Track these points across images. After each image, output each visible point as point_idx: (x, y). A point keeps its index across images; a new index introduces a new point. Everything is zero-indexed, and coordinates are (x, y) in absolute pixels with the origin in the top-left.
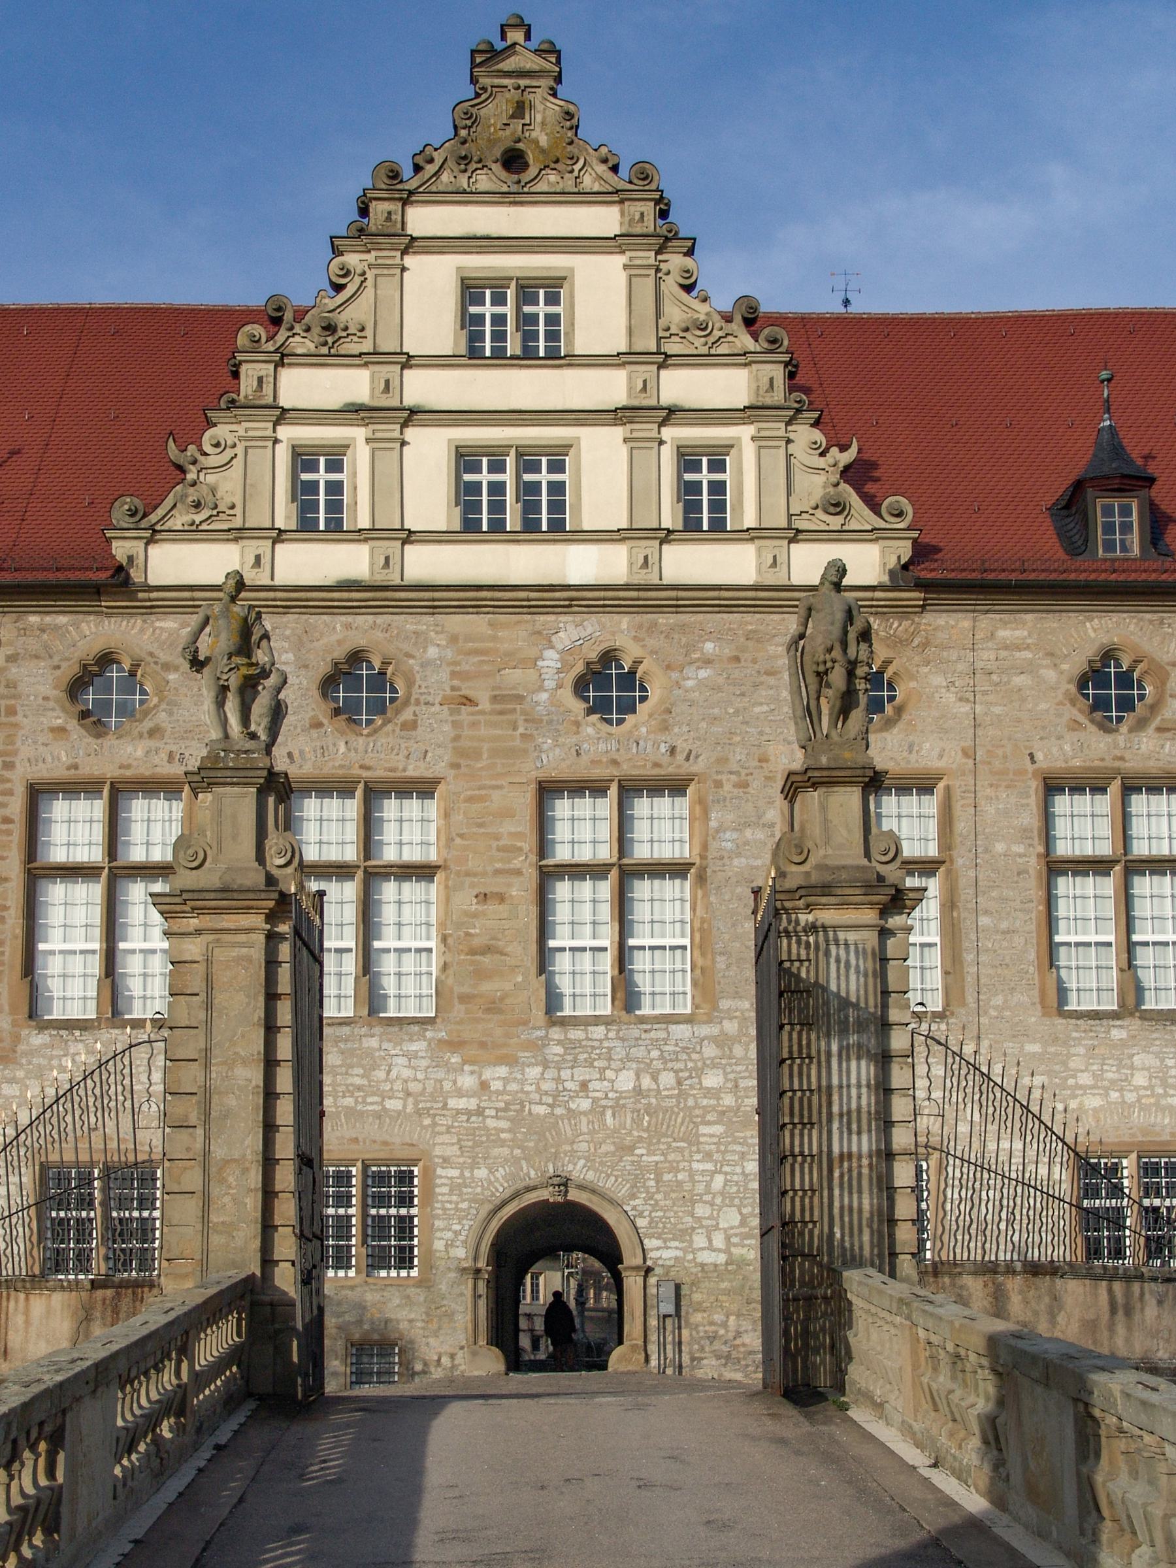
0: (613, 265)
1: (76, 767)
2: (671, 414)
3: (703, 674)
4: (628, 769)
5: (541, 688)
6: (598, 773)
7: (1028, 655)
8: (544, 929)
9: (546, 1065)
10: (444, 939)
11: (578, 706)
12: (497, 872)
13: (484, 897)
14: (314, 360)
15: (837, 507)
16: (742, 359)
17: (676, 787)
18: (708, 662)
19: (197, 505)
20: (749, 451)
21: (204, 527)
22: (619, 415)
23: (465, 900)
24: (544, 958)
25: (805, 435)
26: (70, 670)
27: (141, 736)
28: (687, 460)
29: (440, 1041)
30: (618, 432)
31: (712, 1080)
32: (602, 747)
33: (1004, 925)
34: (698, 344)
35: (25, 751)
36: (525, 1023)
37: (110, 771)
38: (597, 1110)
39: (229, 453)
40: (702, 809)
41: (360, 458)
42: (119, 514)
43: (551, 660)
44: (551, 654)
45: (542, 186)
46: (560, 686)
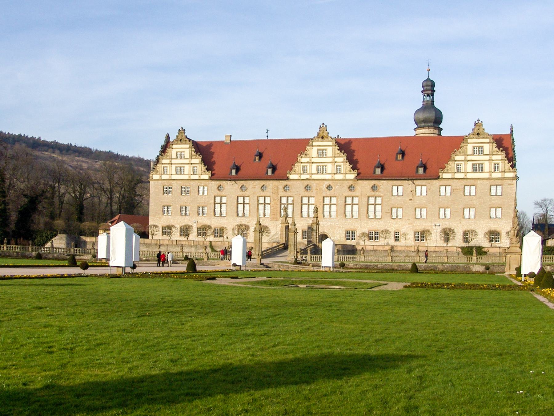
0: (331, 147)
2: (335, 162)
4: (331, 196)
8: (323, 210)
11: (326, 190)
14: (305, 157)
15: (350, 171)
16: (342, 157)
17: (335, 197)
22: (331, 162)
24: (323, 212)
25: (348, 164)
26: (284, 186)
28: (337, 166)
30: (331, 164)
31: (337, 223)
34: (338, 155)
35: (280, 193)
37: (287, 195)
38: (327, 226)
40: (337, 199)
41: (308, 167)
42: (288, 172)
43: (324, 185)
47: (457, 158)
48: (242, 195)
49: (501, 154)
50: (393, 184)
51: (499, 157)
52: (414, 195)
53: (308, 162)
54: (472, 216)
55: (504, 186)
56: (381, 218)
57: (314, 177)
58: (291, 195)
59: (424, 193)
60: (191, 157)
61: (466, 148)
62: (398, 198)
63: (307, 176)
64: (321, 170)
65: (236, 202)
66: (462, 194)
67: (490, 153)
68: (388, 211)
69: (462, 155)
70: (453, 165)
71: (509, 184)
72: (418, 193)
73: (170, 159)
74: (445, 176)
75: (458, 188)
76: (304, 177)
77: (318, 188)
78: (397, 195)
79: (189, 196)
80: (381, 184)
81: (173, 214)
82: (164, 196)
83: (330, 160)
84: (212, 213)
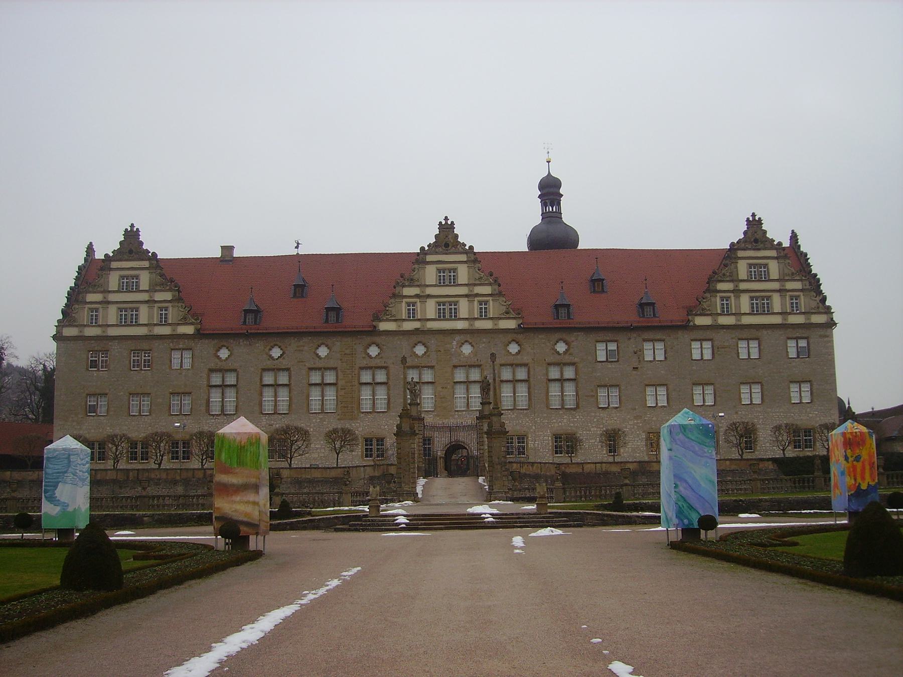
1: (367, 364)
2: (477, 295)
3: (483, 345)
4: (469, 363)
5: (453, 348)
6: (464, 364)
7: (544, 340)
9: (455, 419)
10: (436, 396)
12: (446, 383)
13: (443, 388)
14: (410, 286)
18: (484, 343)
19: (388, 315)
20: (491, 302)
21: (390, 318)
22: (466, 296)
23: (439, 389)
27: (379, 358)
29: (436, 415)
30: (466, 299)
32: (464, 359)
33: (540, 392)
36: (450, 411)
39: (394, 304)
41: (419, 304)
43: (455, 343)
44: (455, 342)
45: (451, 251)
46: (456, 348)
47: (721, 286)
49: (801, 280)
50: (599, 339)
51: (798, 285)
52: (641, 359)
53: (417, 296)
54: (757, 400)
55: (811, 341)
56: (578, 407)
57: (431, 325)
58: (385, 365)
59: (660, 356)
60: (152, 289)
61: (736, 267)
62: (609, 365)
64: (447, 310)
65: (258, 383)
66: (736, 356)
67: (782, 278)
68: (592, 394)
69: (728, 281)
70: (713, 299)
71: (821, 336)
72: (648, 357)
73: (102, 292)
74: (700, 321)
75: (726, 344)
76: (409, 326)
77: (442, 350)
78: (607, 361)
79: (149, 373)
80: (573, 339)
81: (111, 413)
83: (464, 291)
84: (203, 408)
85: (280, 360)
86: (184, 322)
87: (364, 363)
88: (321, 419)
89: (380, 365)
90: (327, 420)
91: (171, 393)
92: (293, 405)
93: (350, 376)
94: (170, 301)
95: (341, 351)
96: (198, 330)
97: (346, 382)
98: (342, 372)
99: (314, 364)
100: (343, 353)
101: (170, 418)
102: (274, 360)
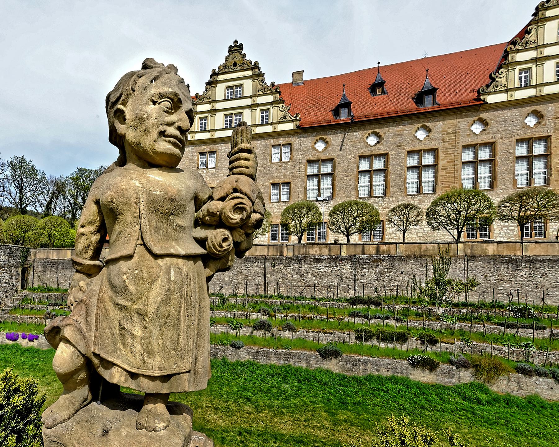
1: (472, 142)
27: (486, 134)
37: (481, 142)
48: (370, 153)
63: (531, 92)
65: (356, 170)
82: (200, 172)
85: (378, 146)
86: (284, 120)
87: (468, 141)
88: (420, 200)
89: (487, 141)
90: (426, 201)
91: (272, 184)
92: (391, 188)
93: (453, 155)
94: (272, 103)
95: (444, 131)
96: (298, 127)
97: (448, 162)
98: (442, 152)
99: (414, 146)
100: (446, 133)
101: (271, 205)
102: (372, 146)
